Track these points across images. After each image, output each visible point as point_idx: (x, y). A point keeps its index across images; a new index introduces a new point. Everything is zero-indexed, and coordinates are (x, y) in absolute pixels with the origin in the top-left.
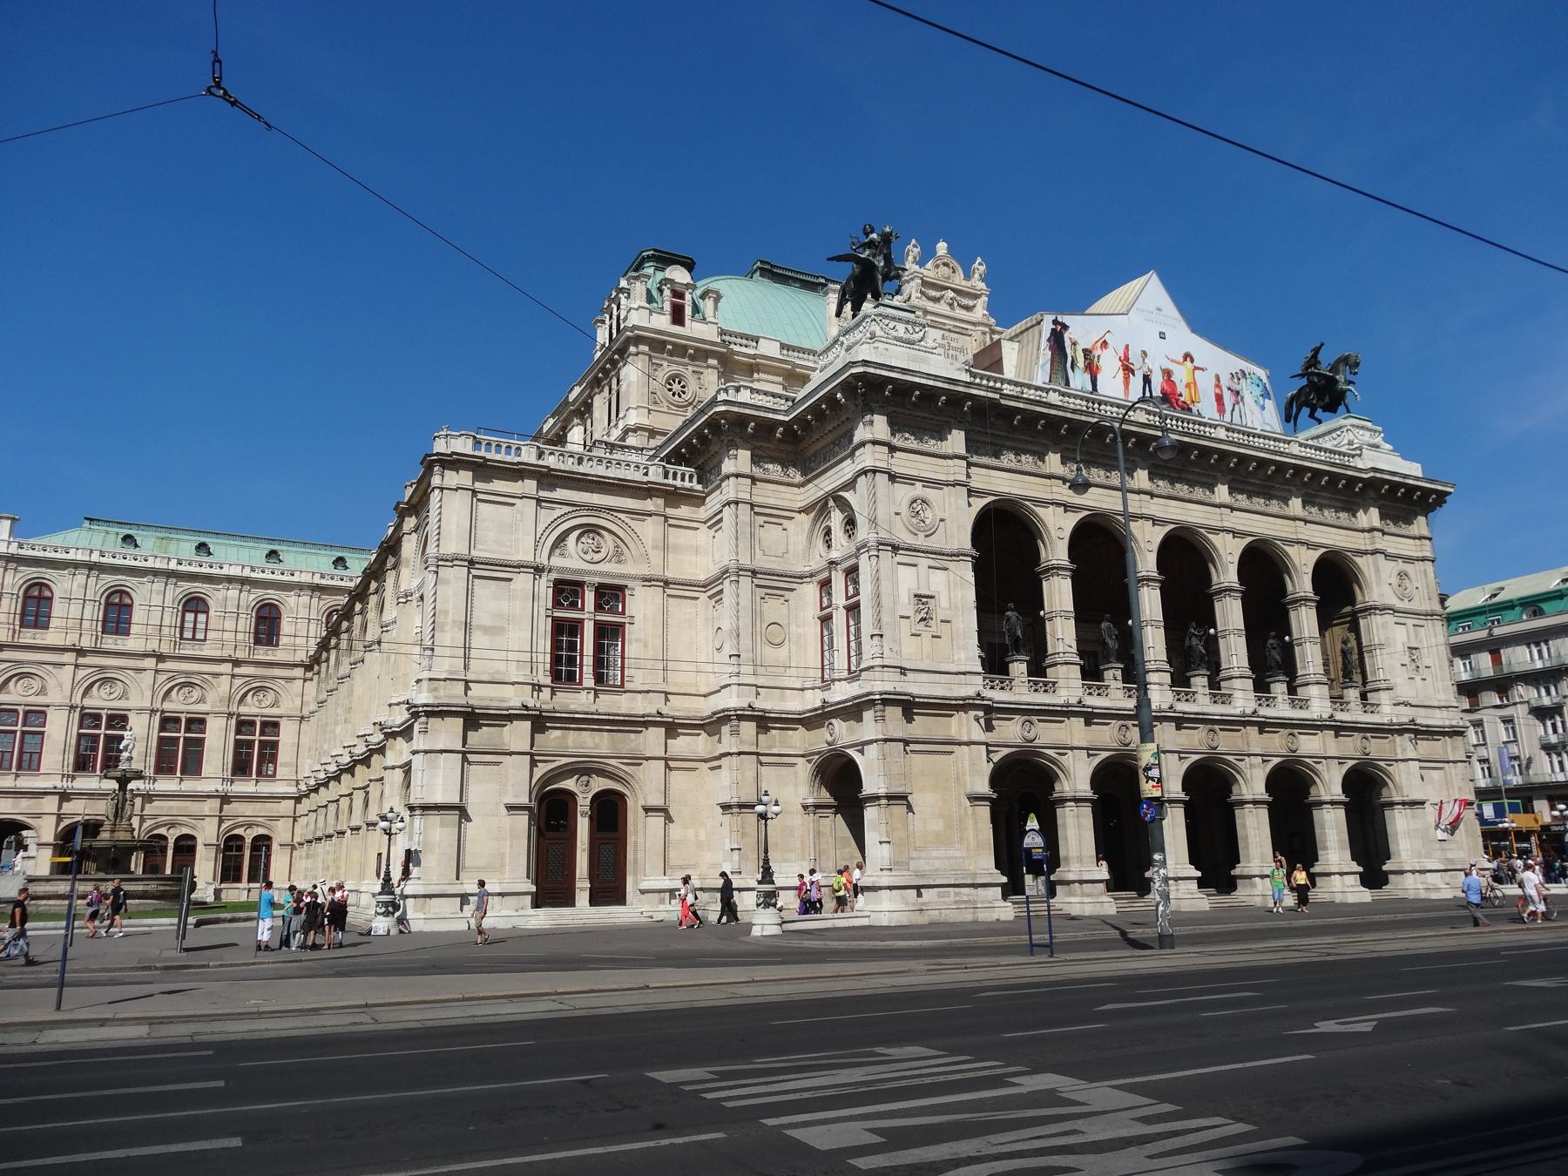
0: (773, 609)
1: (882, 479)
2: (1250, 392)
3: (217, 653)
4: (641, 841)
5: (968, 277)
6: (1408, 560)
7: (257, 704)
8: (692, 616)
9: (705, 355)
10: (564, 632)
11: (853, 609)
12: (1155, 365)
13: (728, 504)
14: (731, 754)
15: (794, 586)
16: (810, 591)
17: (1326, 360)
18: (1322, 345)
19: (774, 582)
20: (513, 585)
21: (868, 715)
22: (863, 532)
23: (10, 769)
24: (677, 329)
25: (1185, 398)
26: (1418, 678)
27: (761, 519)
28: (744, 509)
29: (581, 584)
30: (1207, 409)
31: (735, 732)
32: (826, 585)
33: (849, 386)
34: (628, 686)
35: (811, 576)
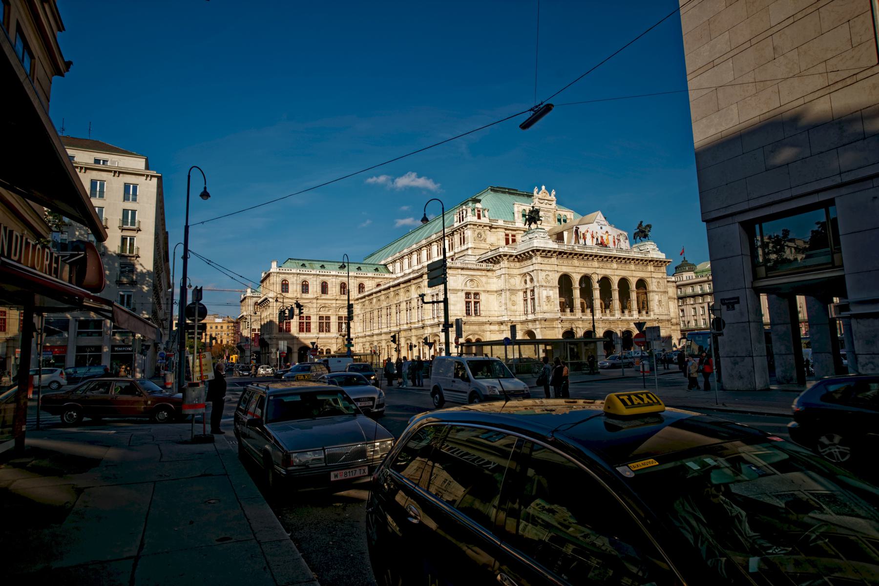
0: (513, 298)
2: (622, 239)
5: (550, 195)
6: (659, 278)
8: (493, 298)
10: (468, 303)
11: (533, 299)
12: (599, 235)
17: (644, 225)
19: (513, 291)
20: (458, 294)
21: (537, 322)
22: (536, 284)
25: (606, 243)
30: (611, 245)
32: (525, 292)
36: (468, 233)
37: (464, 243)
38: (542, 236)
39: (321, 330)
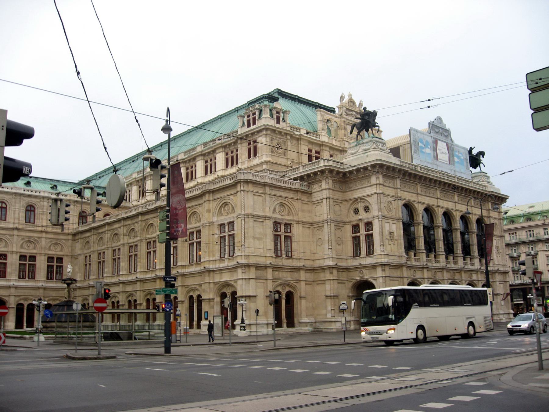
1: (382, 195)
3: (11, 226)
4: (299, 307)
7: (54, 250)
9: (286, 134)
13: (326, 198)
14: (330, 280)
15: (344, 225)
16: (348, 228)
17: (474, 152)
18: (474, 147)
20: (264, 224)
23: (25, 278)
24: (277, 125)
26: (499, 256)
27: (335, 203)
28: (331, 200)
29: (279, 223)
31: (331, 273)
33: (373, 166)
34: (294, 257)
35: (350, 222)
36: (262, 140)
37: (255, 155)
38: (380, 147)
39: (22, 276)
